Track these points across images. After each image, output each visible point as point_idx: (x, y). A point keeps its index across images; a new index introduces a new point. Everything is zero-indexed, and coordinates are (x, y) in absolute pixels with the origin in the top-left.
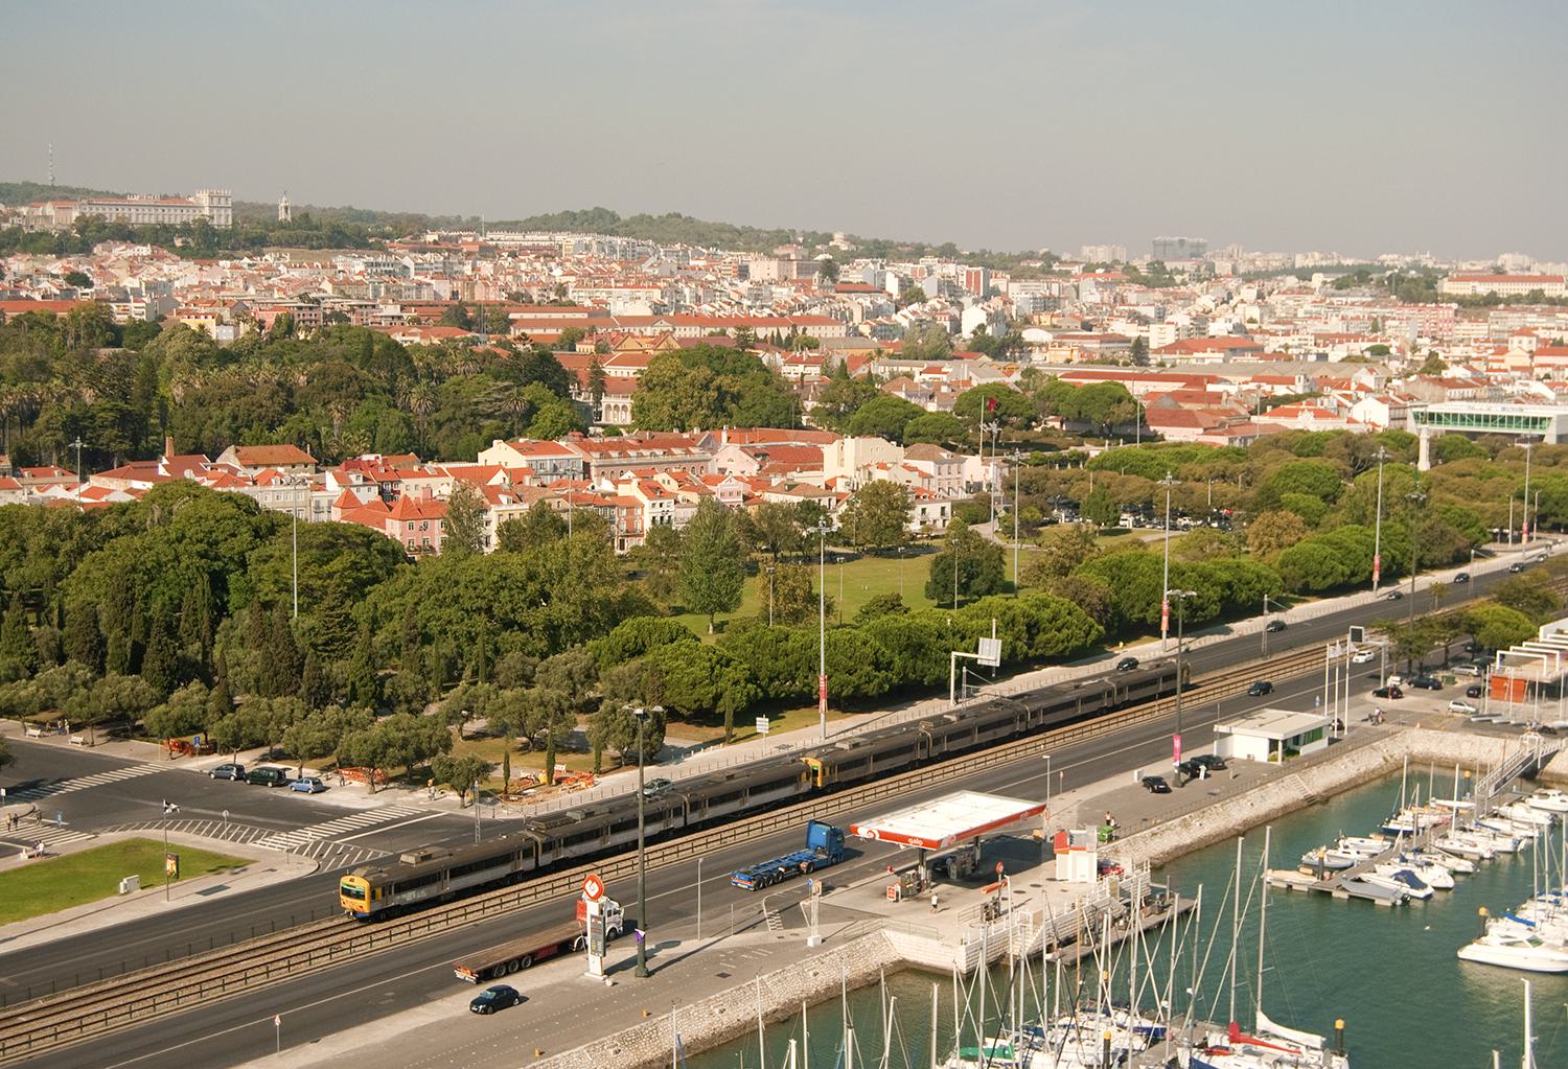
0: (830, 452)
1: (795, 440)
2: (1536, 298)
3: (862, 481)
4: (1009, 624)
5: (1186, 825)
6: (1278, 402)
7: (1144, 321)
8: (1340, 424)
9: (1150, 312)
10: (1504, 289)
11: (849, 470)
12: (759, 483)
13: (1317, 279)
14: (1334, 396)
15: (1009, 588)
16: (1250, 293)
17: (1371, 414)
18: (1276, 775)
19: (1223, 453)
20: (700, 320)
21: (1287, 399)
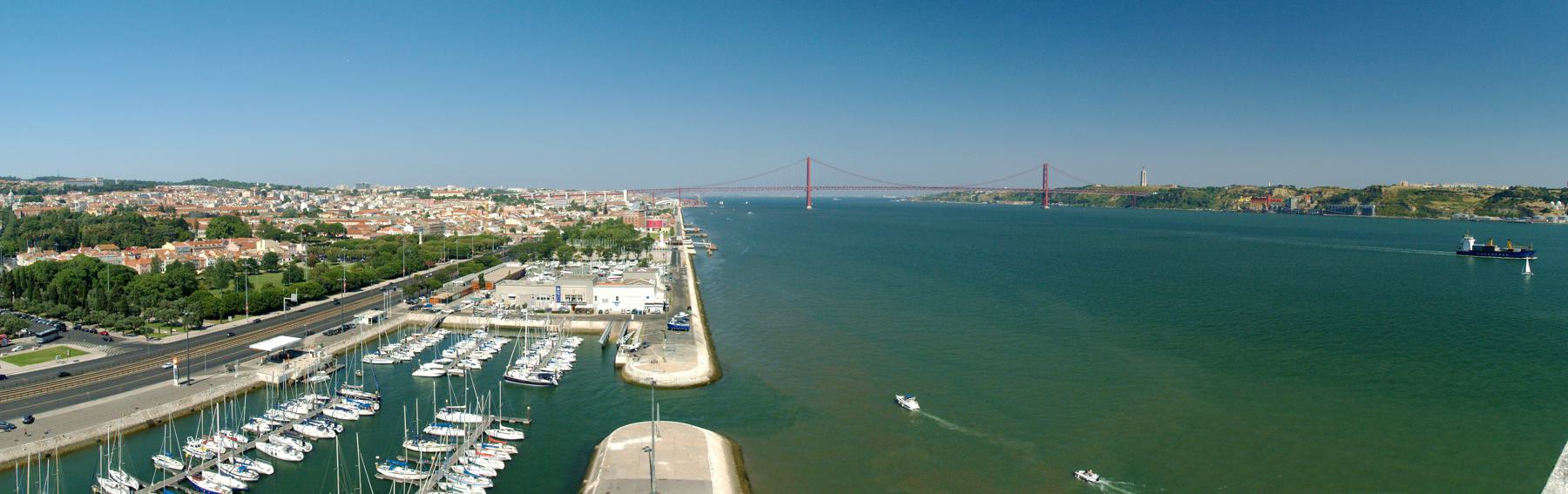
0: (258, 244)
1: (250, 241)
3: (267, 251)
4: (301, 290)
5: (344, 343)
6: (384, 227)
8: (401, 233)
11: (263, 249)
12: (239, 252)
14: (399, 225)
15: (305, 281)
17: (409, 229)
18: (370, 328)
19: (368, 241)
20: (227, 208)
21: (386, 226)
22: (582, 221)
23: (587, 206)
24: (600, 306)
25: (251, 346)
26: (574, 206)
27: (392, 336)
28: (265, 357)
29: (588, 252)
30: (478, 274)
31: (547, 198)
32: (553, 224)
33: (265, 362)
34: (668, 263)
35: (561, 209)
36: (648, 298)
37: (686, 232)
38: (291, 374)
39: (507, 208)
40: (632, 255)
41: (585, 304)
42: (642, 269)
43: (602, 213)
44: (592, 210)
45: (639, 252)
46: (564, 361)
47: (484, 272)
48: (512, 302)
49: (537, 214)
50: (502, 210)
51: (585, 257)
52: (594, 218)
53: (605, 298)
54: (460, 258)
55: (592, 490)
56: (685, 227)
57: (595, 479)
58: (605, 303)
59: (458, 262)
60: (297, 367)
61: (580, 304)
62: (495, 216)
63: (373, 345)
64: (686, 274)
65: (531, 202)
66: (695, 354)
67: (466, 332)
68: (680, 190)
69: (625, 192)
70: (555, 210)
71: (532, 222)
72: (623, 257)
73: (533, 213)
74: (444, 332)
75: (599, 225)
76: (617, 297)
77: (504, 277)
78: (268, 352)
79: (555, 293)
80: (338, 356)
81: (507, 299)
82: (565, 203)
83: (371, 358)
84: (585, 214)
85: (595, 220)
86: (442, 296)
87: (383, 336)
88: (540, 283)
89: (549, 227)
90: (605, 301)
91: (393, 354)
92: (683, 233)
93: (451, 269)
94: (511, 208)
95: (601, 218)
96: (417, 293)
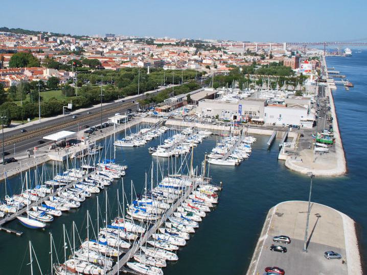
0: (44, 71)
1: (39, 69)
2: (170, 44)
4: (74, 102)
6: (125, 62)
7: (103, 48)
9: (104, 47)
10: (165, 43)
12: (32, 77)
13: (133, 41)
14: (134, 61)
16: (122, 43)
19: (115, 71)
22: (255, 63)
23: (257, 53)
24: (269, 121)
25: (44, 138)
26: (249, 53)
27: (134, 129)
28: (53, 144)
29: (260, 83)
30: (187, 94)
31: (230, 47)
32: (235, 64)
33: (53, 148)
34: (316, 95)
35: (240, 54)
36: (302, 117)
37: (329, 73)
38: (71, 154)
39: (204, 52)
40: (290, 87)
41: (258, 118)
42: (299, 97)
43: (268, 57)
44: (260, 55)
45: (295, 85)
46: (243, 152)
47: (191, 93)
48: (209, 114)
49: (224, 57)
50: (200, 54)
51: (257, 87)
52: (263, 61)
53: (275, 116)
54: (174, 84)
55: (262, 242)
56: (328, 69)
57: (265, 234)
58: (271, 119)
59: (173, 86)
60: (73, 151)
61: (254, 117)
62: (196, 57)
63: (121, 135)
64: (329, 103)
65: (220, 49)
66: (336, 159)
67: (178, 130)
68: (325, 44)
69: (285, 44)
70: (236, 55)
71: (220, 62)
72: (284, 87)
73: (221, 56)
74: (165, 128)
75: (267, 66)
76: (280, 115)
77: (204, 97)
78: (55, 141)
79: (238, 110)
80: (101, 142)
81: (205, 111)
82: (242, 51)
83: (119, 143)
84: (257, 58)
85: (264, 62)
86: (164, 108)
87: (128, 129)
88: (228, 102)
89: (233, 66)
90: (272, 117)
91: (136, 141)
92: (327, 74)
93: (170, 90)
94: (207, 53)
95: (267, 61)
96: (150, 103)
